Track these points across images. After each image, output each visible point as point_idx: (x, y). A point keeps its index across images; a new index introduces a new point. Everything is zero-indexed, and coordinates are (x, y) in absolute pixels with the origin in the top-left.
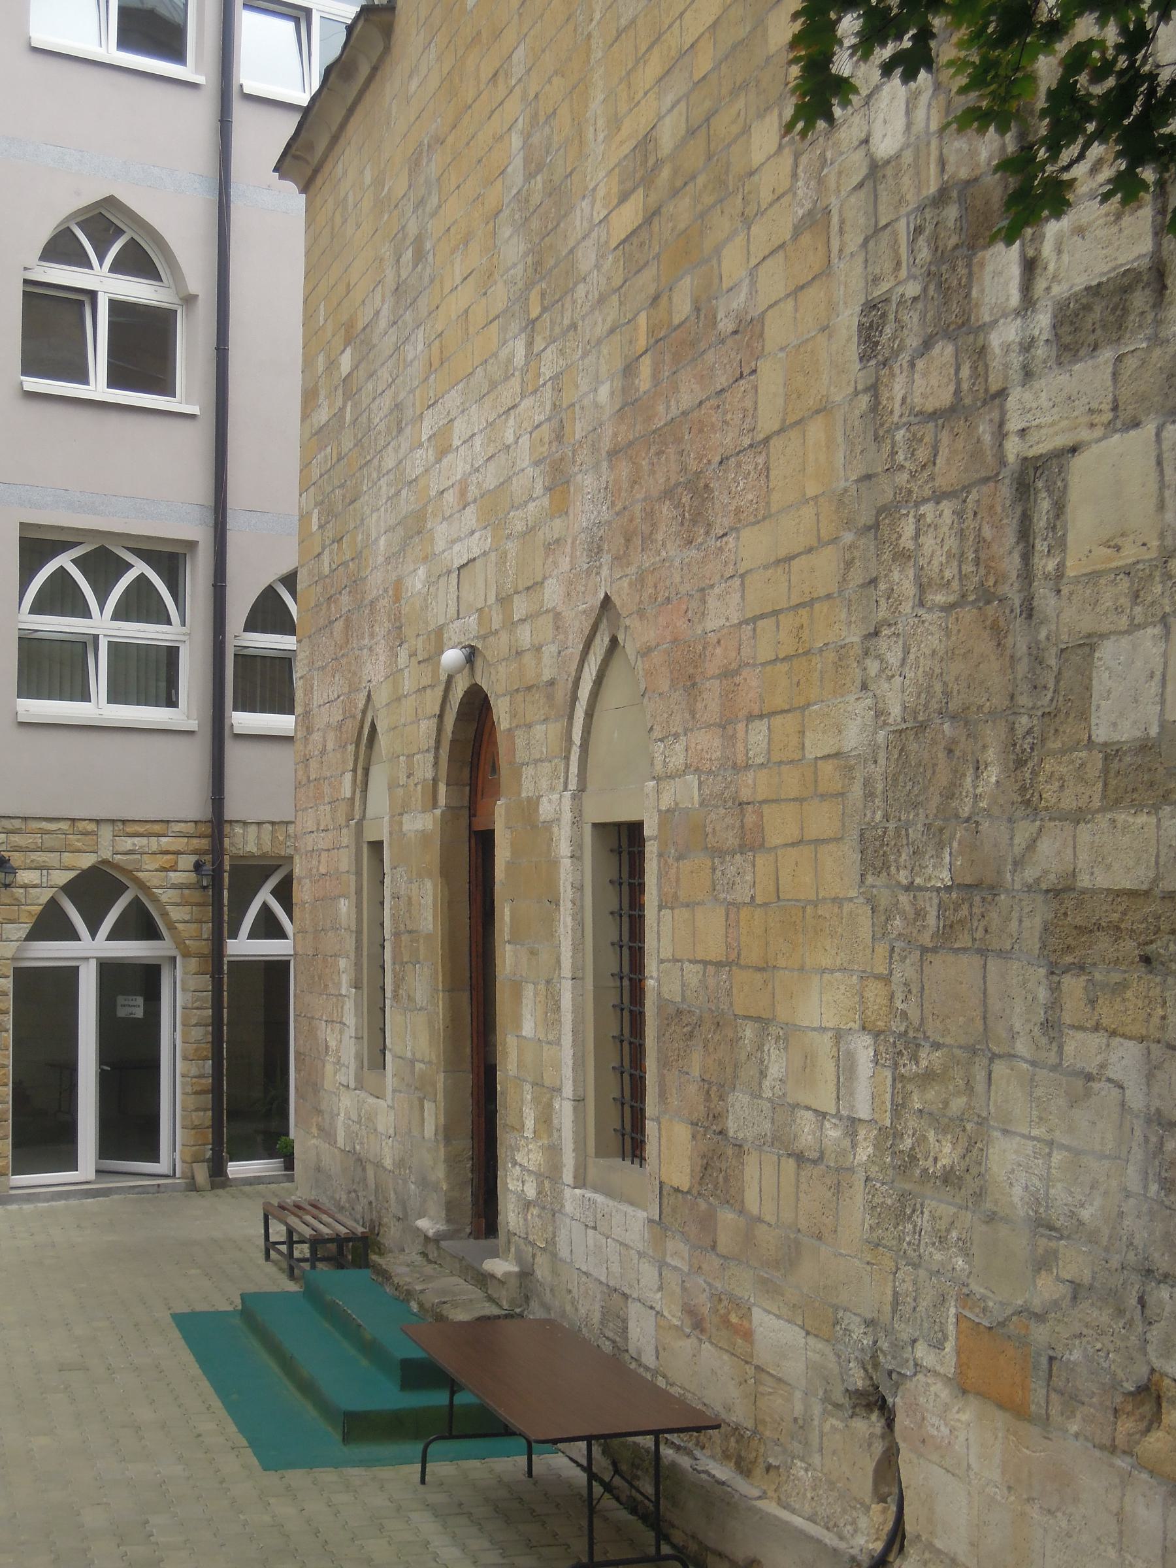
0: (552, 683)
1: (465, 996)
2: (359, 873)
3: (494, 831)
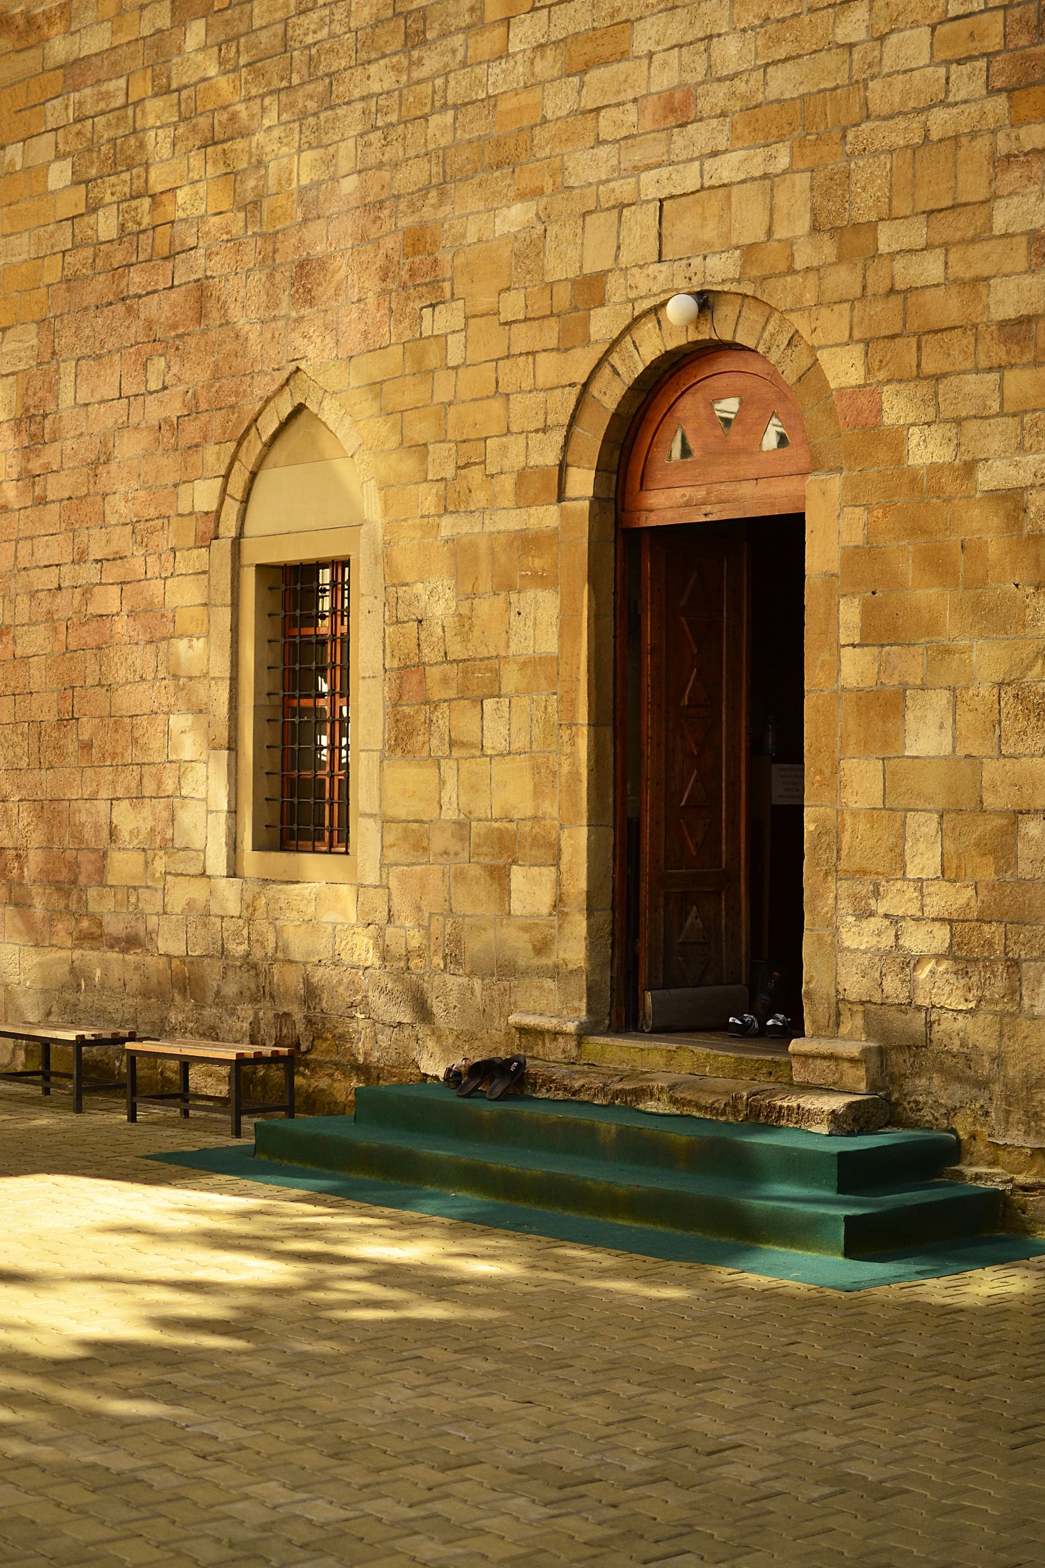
0: (1025, 321)
1: (609, 732)
2: (235, 605)
3: (804, 514)
